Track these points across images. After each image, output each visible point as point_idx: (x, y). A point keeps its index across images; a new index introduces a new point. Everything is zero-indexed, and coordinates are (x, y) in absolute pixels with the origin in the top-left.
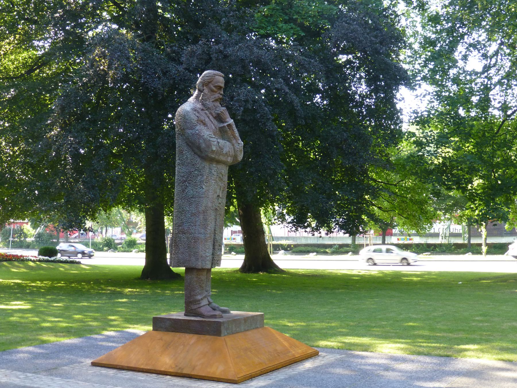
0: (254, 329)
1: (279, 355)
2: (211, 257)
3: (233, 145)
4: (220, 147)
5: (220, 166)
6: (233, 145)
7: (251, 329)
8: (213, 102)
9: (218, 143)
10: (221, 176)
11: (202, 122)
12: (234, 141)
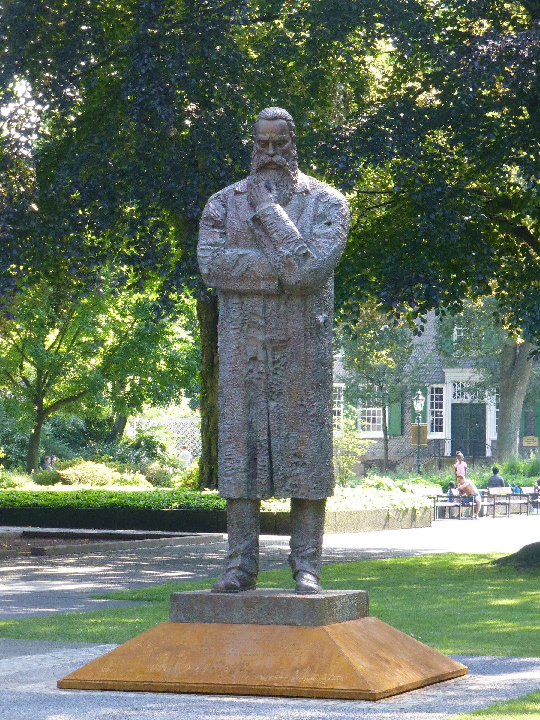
0: (277, 624)
1: (232, 673)
2: (242, 478)
3: (267, 256)
4: (219, 267)
5: (249, 302)
6: (267, 256)
7: (268, 624)
8: (257, 172)
9: (214, 258)
10: (253, 318)
11: (212, 219)
12: (269, 250)
